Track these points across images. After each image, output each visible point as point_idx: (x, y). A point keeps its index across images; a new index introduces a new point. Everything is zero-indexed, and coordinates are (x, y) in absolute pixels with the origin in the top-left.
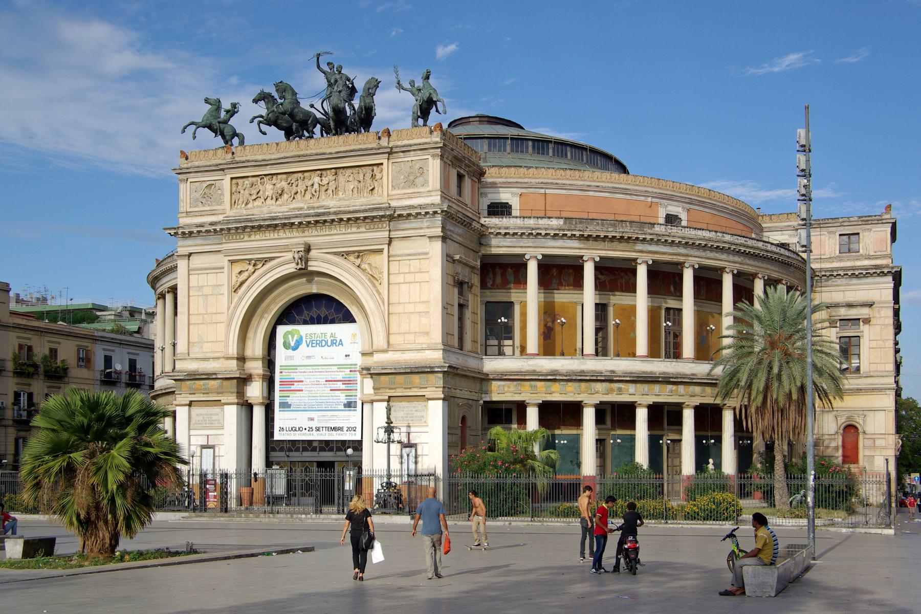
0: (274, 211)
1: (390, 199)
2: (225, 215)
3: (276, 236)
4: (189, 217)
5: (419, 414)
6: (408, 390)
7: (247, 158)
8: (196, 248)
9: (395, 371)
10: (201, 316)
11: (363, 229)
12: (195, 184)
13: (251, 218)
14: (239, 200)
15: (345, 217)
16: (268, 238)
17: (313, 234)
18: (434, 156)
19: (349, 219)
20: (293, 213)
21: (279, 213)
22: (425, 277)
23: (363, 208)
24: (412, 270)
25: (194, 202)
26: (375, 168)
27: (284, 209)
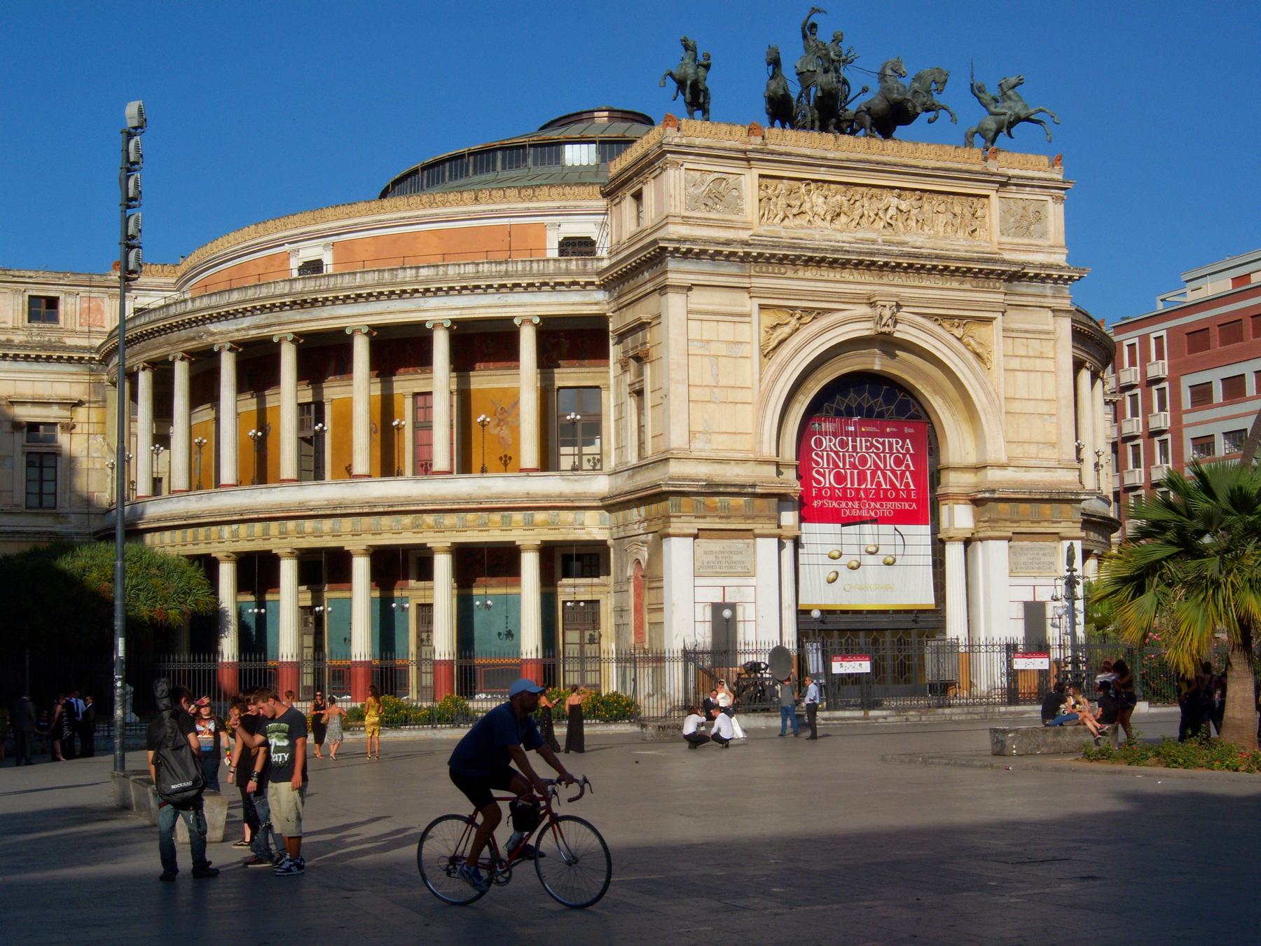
0: (833, 238)
1: (1000, 249)
2: (751, 232)
3: (838, 277)
5: (1047, 559)
6: (1036, 525)
7: (788, 149)
8: (701, 277)
9: (1028, 497)
10: (707, 390)
12: (692, 172)
15: (953, 265)
16: (825, 278)
17: (895, 282)
18: (1056, 199)
22: (1050, 365)
23: (968, 255)
24: (1031, 354)
25: (693, 202)
26: (975, 200)
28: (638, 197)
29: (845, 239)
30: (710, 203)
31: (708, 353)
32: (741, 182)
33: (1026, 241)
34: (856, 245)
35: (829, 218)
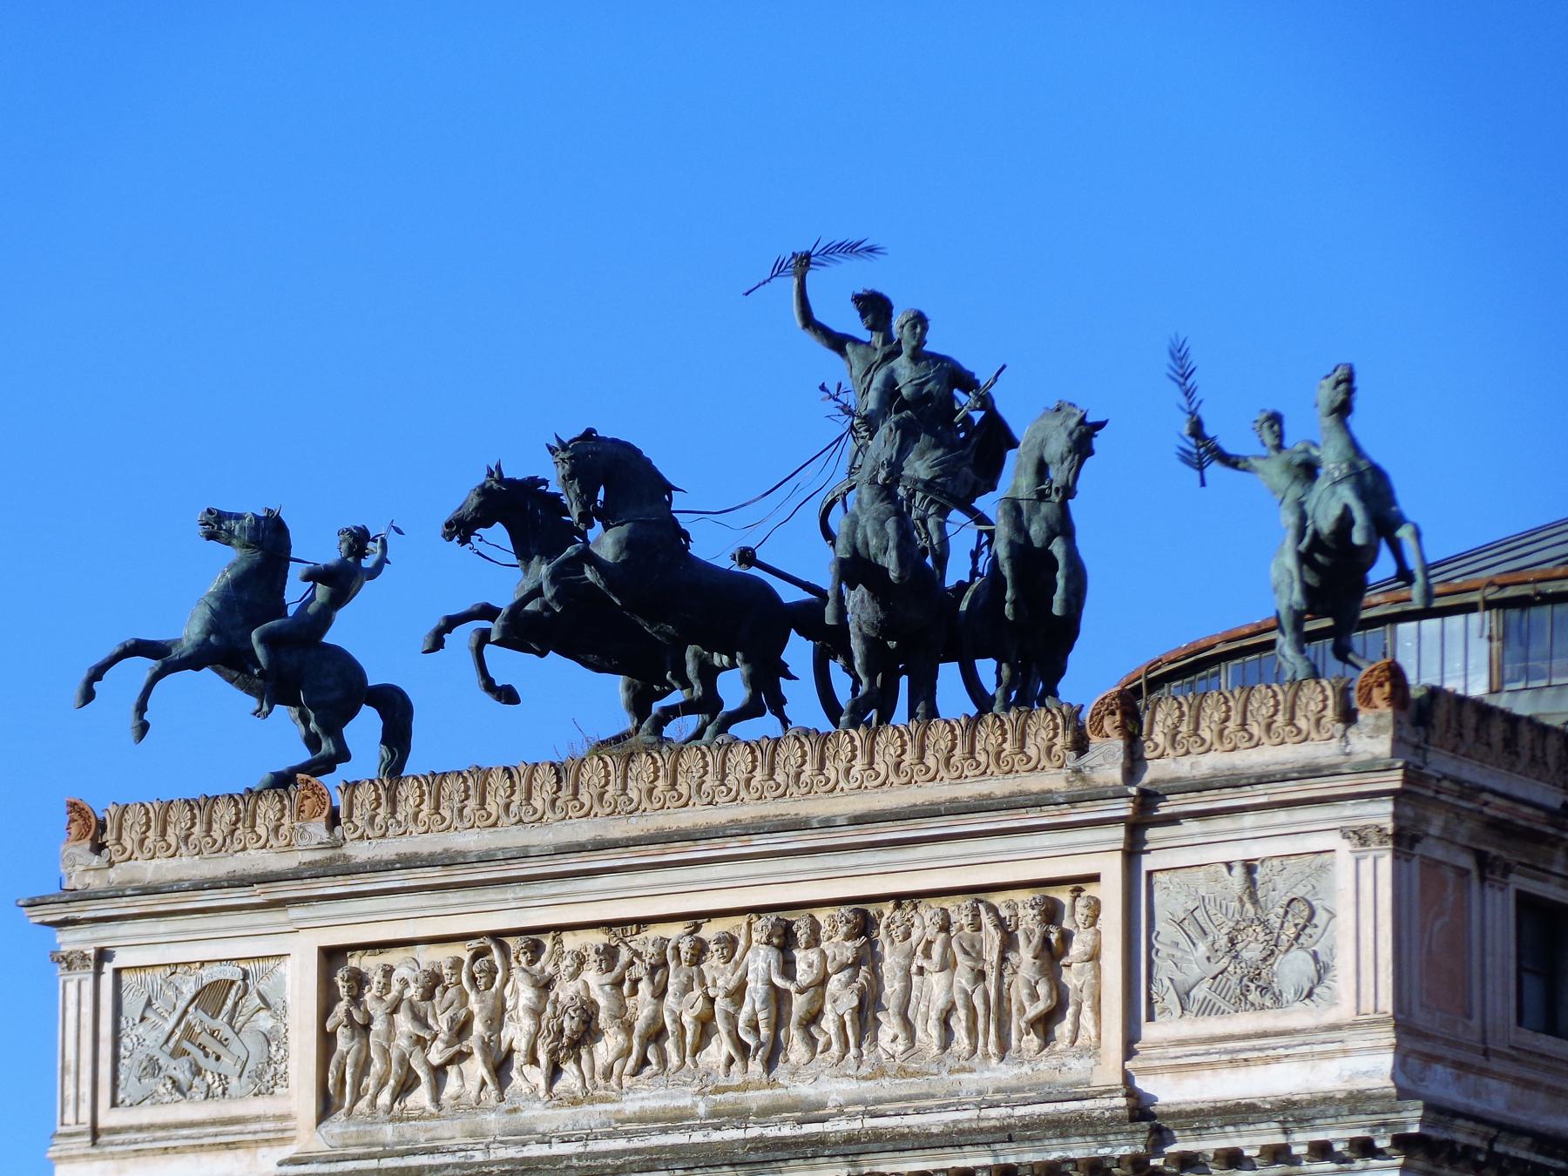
2: (289, 1151)
4: (103, 1156)
14: (363, 1067)
18: (1360, 837)
20: (637, 1143)
21: (564, 1140)
27: (591, 1115)
32: (283, 976)
33: (1245, 1022)
35: (543, 1057)
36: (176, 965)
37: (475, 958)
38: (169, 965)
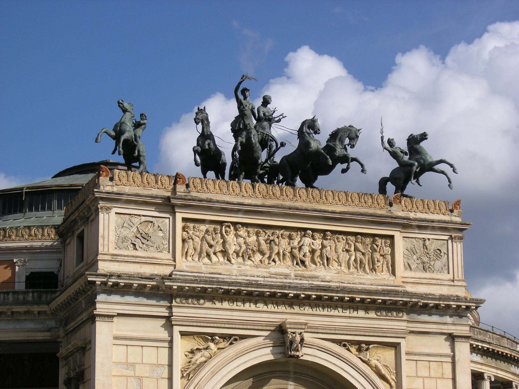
0: (249, 273)
1: (403, 282)
3: (253, 307)
11: (372, 314)
12: (122, 216)
13: (217, 278)
19: (363, 300)
23: (374, 288)
24: (433, 374)
27: (262, 271)
28: (81, 238)
29: (259, 274)
30: (138, 243)
31: (131, 373)
33: (427, 275)
34: (270, 279)
36: (134, 215)
37: (225, 227)
38: (132, 214)
